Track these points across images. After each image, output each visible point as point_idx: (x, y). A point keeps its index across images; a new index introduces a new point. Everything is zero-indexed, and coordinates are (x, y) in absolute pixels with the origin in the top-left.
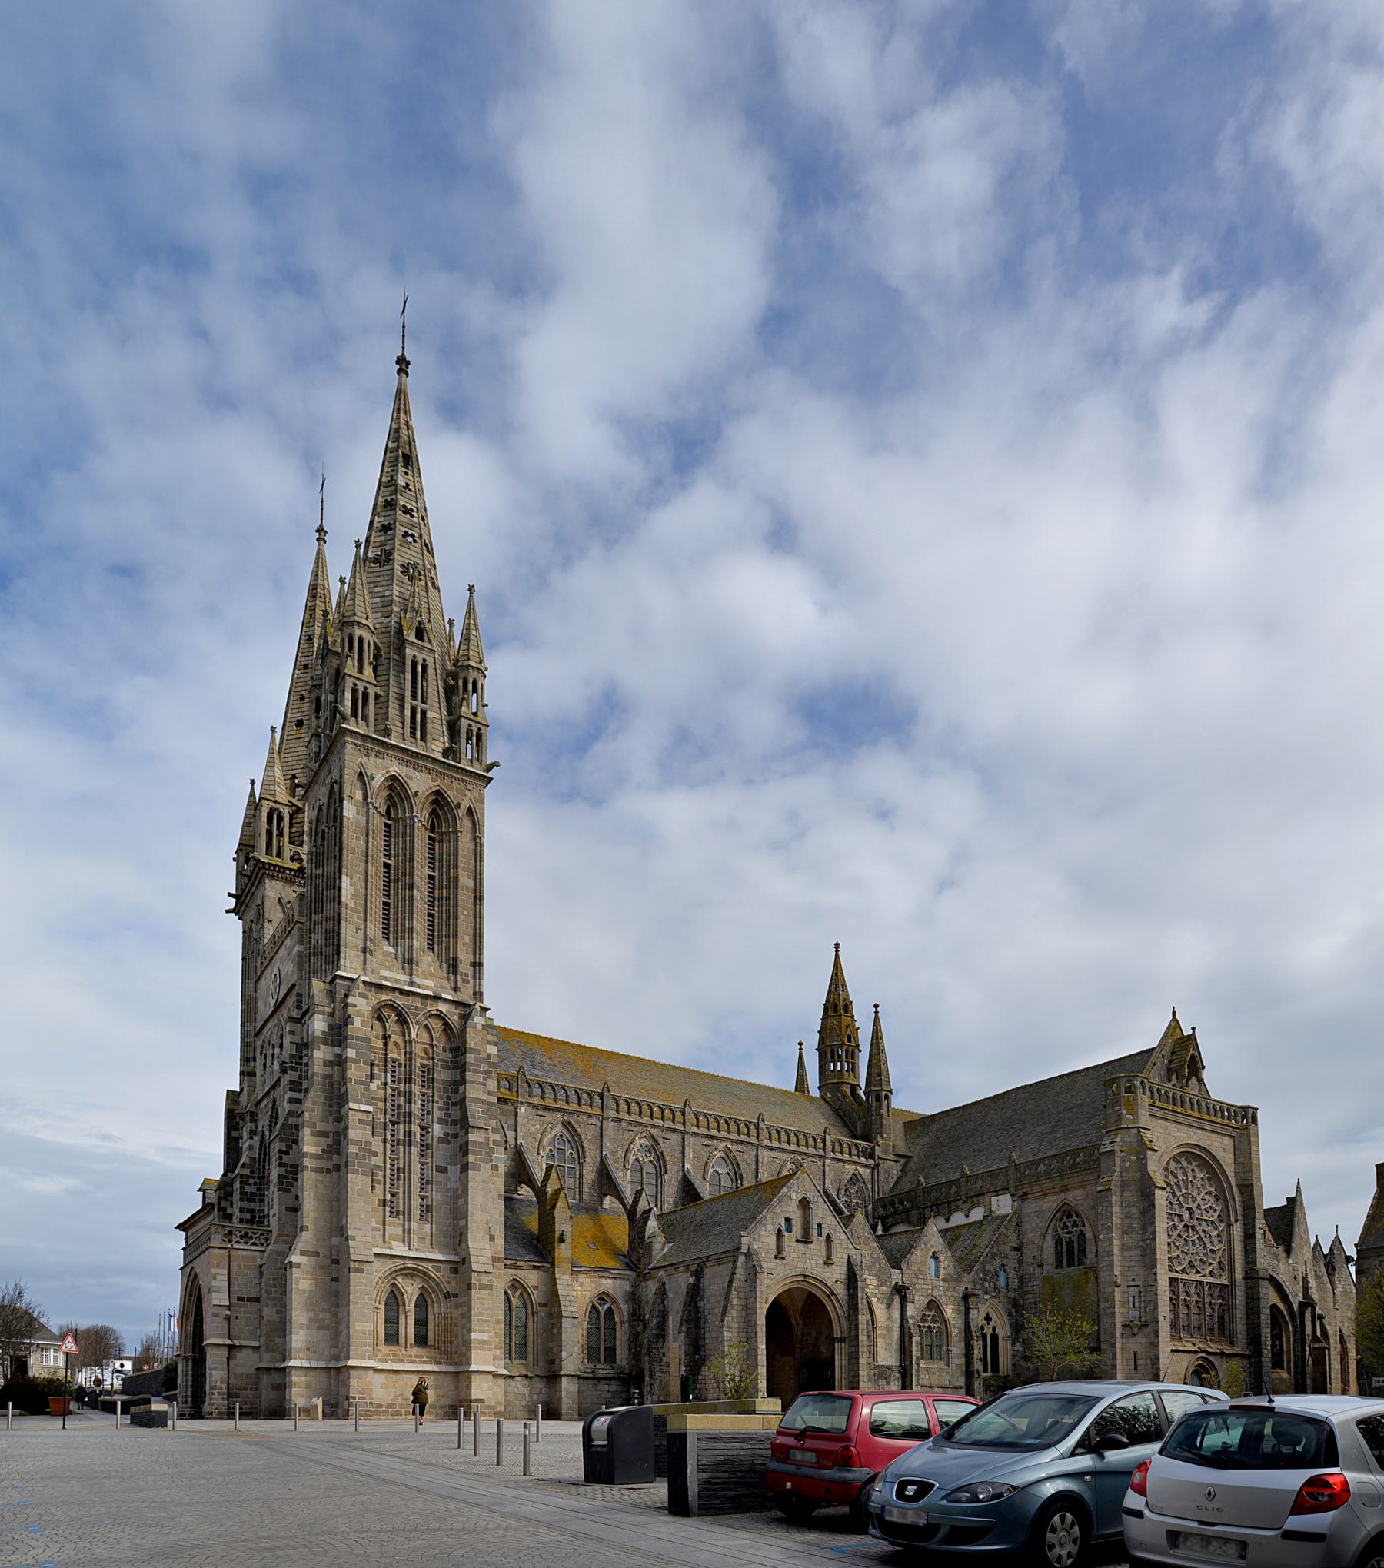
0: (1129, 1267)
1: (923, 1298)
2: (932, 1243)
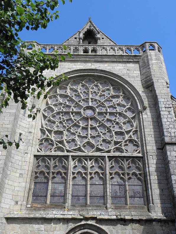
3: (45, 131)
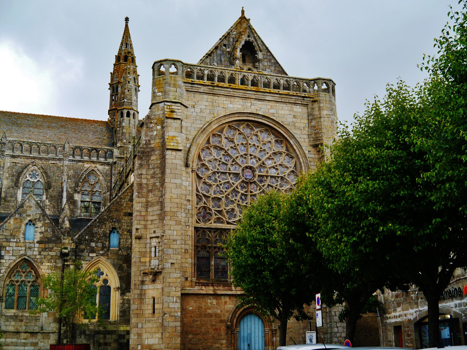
0: (152, 221)
1: (14, 258)
2: (29, 212)
3: (201, 196)
